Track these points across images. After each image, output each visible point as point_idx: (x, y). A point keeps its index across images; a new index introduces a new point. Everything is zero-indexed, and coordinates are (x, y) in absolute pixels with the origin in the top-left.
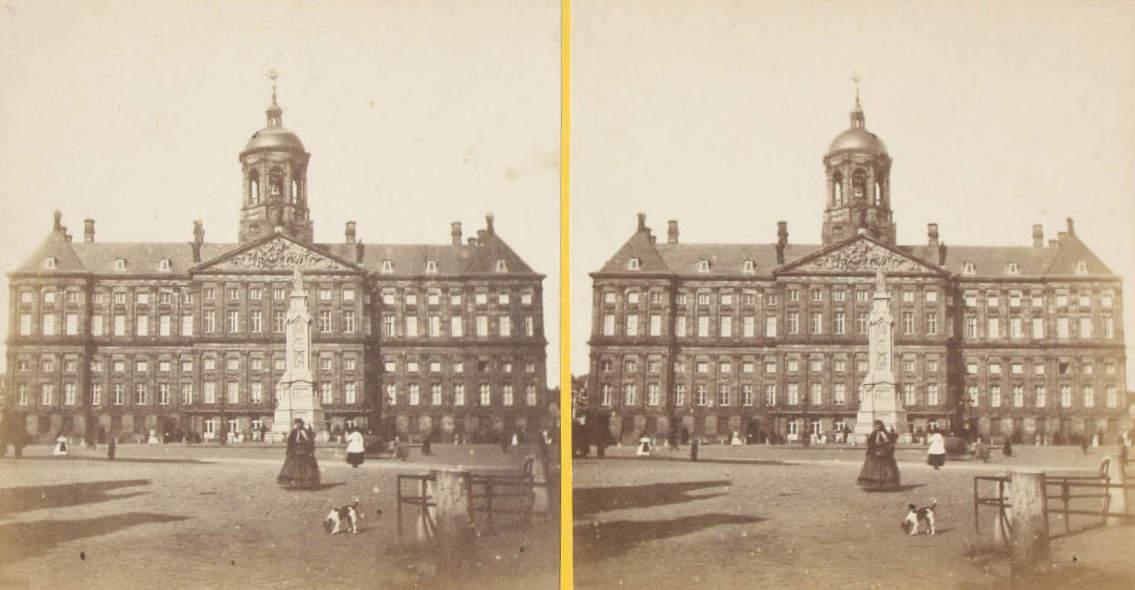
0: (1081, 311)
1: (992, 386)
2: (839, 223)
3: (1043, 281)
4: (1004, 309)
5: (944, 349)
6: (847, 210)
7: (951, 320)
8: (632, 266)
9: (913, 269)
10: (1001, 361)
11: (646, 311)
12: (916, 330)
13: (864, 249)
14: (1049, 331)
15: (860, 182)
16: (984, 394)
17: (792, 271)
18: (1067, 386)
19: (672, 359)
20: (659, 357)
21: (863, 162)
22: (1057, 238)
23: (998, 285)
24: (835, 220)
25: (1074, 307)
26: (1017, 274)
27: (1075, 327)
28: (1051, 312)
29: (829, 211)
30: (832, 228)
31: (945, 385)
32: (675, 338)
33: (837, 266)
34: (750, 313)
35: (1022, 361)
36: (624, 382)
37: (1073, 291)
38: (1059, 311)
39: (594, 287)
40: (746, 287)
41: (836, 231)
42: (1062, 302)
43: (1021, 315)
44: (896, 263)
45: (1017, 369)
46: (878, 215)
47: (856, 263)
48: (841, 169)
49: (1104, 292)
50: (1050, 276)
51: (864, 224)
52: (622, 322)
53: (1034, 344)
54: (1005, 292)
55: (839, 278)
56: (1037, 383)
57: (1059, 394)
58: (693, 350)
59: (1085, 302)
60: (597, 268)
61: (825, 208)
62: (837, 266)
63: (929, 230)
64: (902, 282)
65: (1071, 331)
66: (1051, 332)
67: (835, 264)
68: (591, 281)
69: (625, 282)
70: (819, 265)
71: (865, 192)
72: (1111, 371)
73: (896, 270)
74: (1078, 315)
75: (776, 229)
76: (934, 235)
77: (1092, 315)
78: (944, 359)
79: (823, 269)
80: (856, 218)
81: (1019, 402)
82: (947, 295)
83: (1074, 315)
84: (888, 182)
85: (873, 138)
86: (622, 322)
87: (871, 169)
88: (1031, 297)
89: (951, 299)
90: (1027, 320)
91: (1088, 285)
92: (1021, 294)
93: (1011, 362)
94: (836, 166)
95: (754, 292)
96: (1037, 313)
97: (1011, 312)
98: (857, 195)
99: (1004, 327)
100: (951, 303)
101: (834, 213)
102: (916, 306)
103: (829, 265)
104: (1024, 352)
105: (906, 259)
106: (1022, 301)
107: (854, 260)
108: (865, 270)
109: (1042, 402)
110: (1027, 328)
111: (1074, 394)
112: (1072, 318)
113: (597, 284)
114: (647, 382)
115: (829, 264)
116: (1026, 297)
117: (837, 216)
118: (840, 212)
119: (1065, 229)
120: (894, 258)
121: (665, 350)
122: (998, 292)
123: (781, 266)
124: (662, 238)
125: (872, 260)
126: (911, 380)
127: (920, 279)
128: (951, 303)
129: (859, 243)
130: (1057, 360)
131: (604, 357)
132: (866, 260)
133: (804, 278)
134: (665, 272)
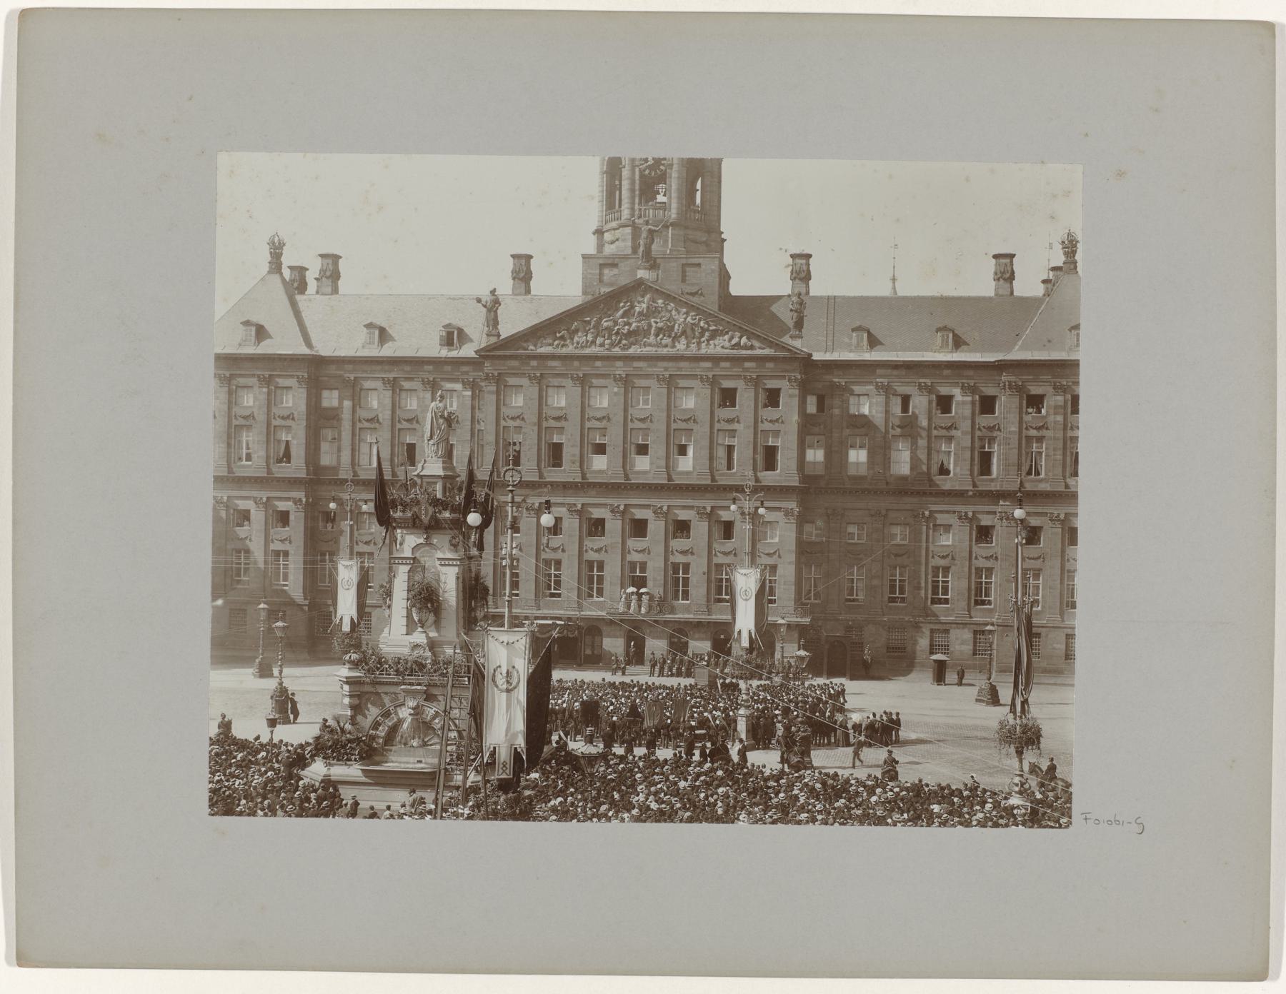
2: (613, 257)
5: (793, 505)
6: (628, 230)
9: (738, 344)
13: (644, 306)
20: (290, 503)
24: (609, 250)
29: (599, 232)
30: (599, 264)
33: (593, 342)
40: (443, 379)
41: (606, 271)
47: (630, 333)
50: (1017, 355)
55: (598, 364)
62: (593, 342)
63: (794, 265)
64: (718, 372)
67: (590, 338)
70: (562, 338)
73: (703, 351)
76: (802, 274)
79: (570, 349)
95: (458, 386)
101: (607, 237)
119: (1059, 260)
120: (702, 324)
125: (659, 331)
133: (534, 363)
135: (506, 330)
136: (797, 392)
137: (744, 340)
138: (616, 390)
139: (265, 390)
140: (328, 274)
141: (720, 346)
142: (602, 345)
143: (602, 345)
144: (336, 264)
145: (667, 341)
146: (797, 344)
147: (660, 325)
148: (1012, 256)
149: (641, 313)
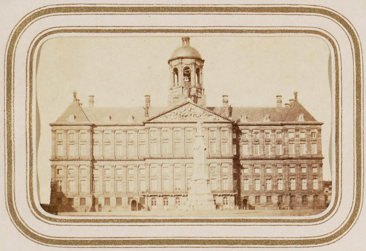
0: (301, 140)
1: (256, 180)
3: (282, 125)
4: (262, 140)
5: (231, 161)
6: (182, 88)
7: (235, 146)
8: (71, 120)
10: (260, 167)
11: (79, 143)
12: (217, 152)
14: (285, 151)
15: (187, 74)
16: (252, 184)
17: (152, 121)
18: (293, 179)
19: (93, 167)
21: (189, 63)
22: (289, 102)
23: (259, 127)
25: (297, 138)
26: (268, 121)
27: (297, 148)
28: (286, 141)
31: (232, 179)
32: (93, 157)
34: (131, 143)
35: (271, 167)
36: (68, 179)
37: (297, 130)
38: (290, 141)
39: (52, 131)
41: (175, 100)
42: (291, 136)
43: (271, 143)
44: (207, 116)
45: (269, 171)
46: (197, 91)
47: (186, 116)
48: (177, 67)
49: (312, 131)
51: (190, 96)
52: (67, 149)
53: (277, 158)
54: (263, 131)
56: (278, 177)
57: (290, 184)
58: (102, 163)
59: (303, 136)
60: (53, 121)
61: (170, 89)
65: (296, 151)
66: (286, 151)
68: (51, 127)
69: (68, 127)
71: (190, 79)
72: (315, 171)
74: (300, 142)
75: (144, 99)
77: (306, 142)
78: (232, 166)
80: (186, 93)
81: (269, 188)
82: (233, 133)
83: (297, 143)
84: (201, 73)
85: (194, 51)
86: (67, 149)
87: (193, 67)
88: (275, 133)
89: (235, 135)
90: (274, 146)
91: (304, 127)
92: (270, 131)
93: (266, 167)
94: (175, 66)
95: (133, 132)
96: (279, 142)
97: (266, 141)
98: (186, 80)
99: (262, 149)
100: (235, 137)
101: (174, 90)
102: (217, 139)
103: (171, 117)
104: (272, 162)
105: (212, 114)
106: (271, 135)
107: (185, 115)
108: (191, 121)
109: (281, 187)
110: (274, 149)
111: (297, 183)
112: (296, 144)
113: (53, 129)
114: (80, 179)
115: (172, 117)
116: (273, 134)
117: (176, 92)
118: (177, 89)
119: (293, 97)
121: (89, 163)
122: (259, 131)
123: (147, 119)
124: (85, 105)
126: (215, 177)
127: (219, 125)
128: (235, 137)
129: (187, 105)
130: (289, 165)
131: (58, 167)
132: (191, 115)
134: (88, 123)
135: (151, 116)
136: (231, 131)
137: (218, 118)
138: (182, 131)
139: (78, 134)
140: (91, 101)
141: (212, 118)
142: (179, 119)
143: (179, 119)
144: (93, 99)
145: (196, 118)
146: (231, 118)
147: (195, 114)
148: (281, 96)
149: (189, 111)
